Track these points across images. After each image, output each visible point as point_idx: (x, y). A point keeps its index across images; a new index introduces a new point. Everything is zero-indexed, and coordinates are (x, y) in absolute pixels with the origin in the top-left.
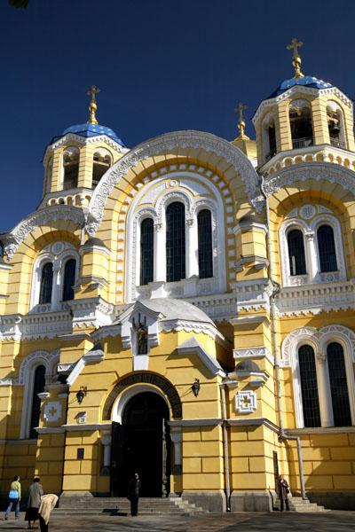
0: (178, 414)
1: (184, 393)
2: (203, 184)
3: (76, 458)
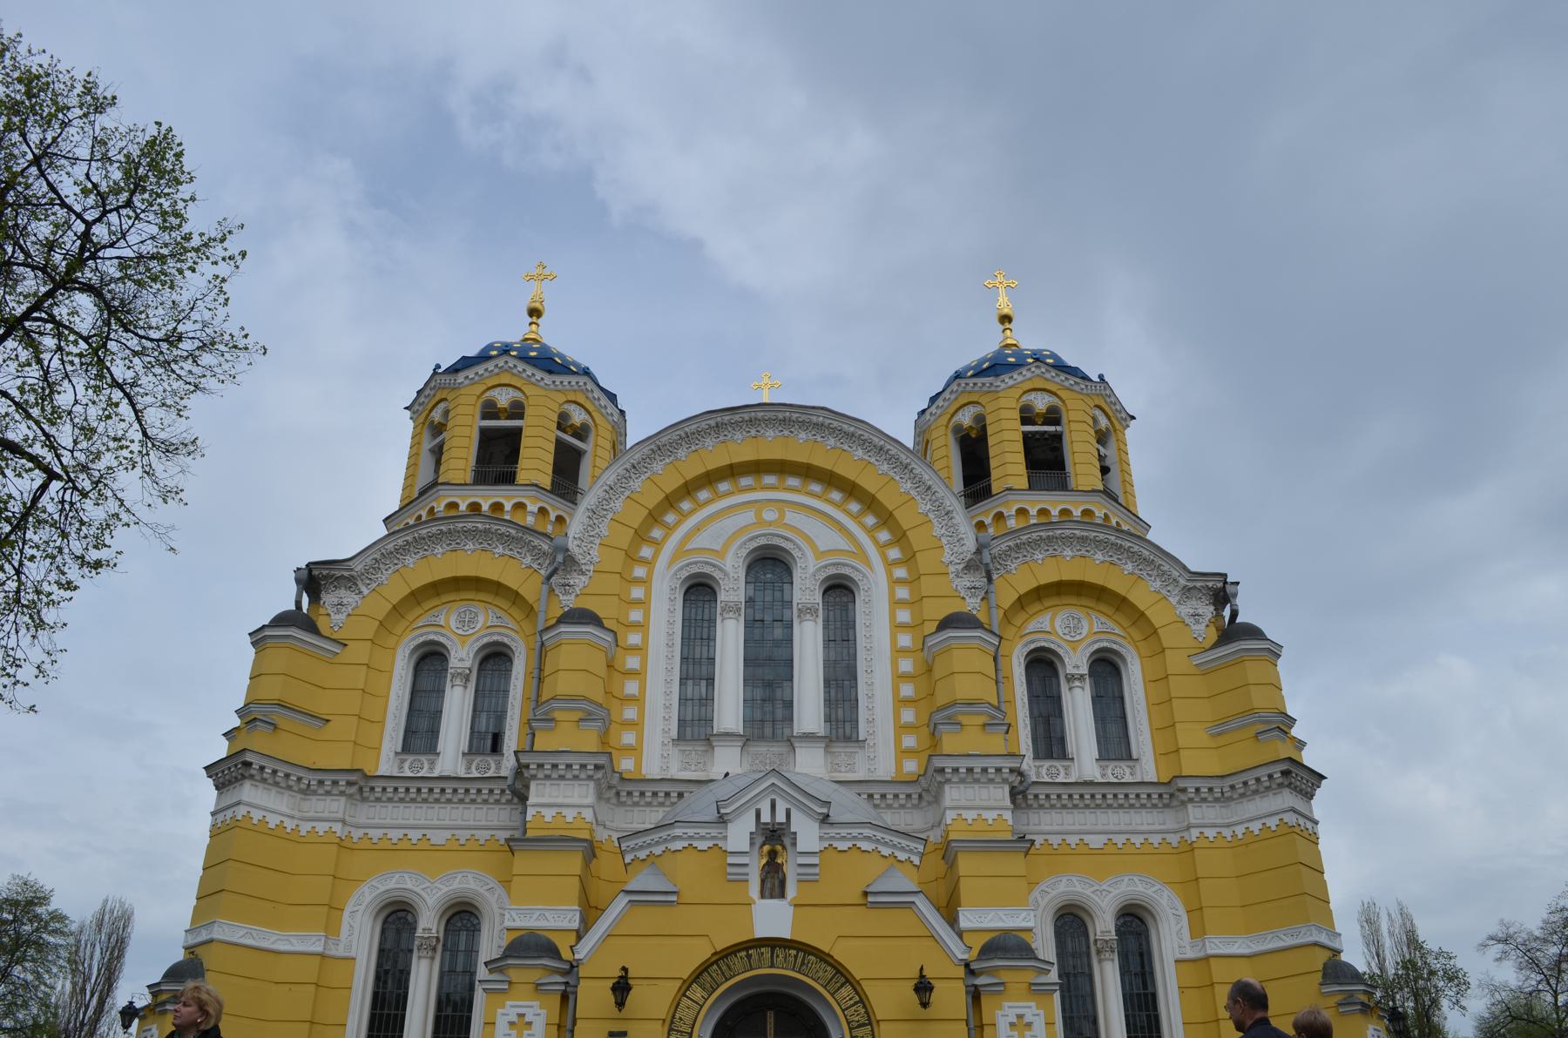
2: (842, 528)
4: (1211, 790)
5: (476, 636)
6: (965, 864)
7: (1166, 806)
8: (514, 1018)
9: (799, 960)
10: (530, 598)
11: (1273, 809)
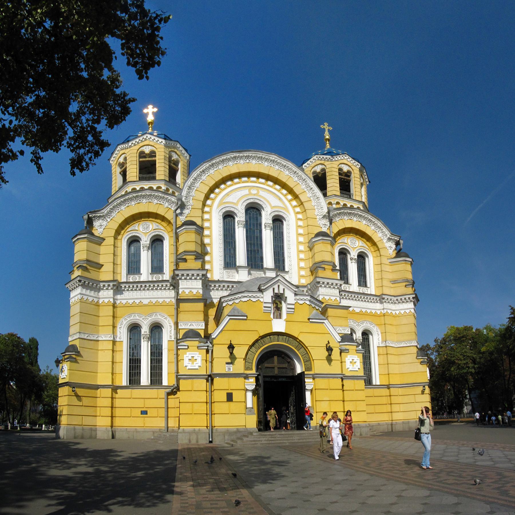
5: (150, 233)
8: (190, 358)
9: (287, 340)
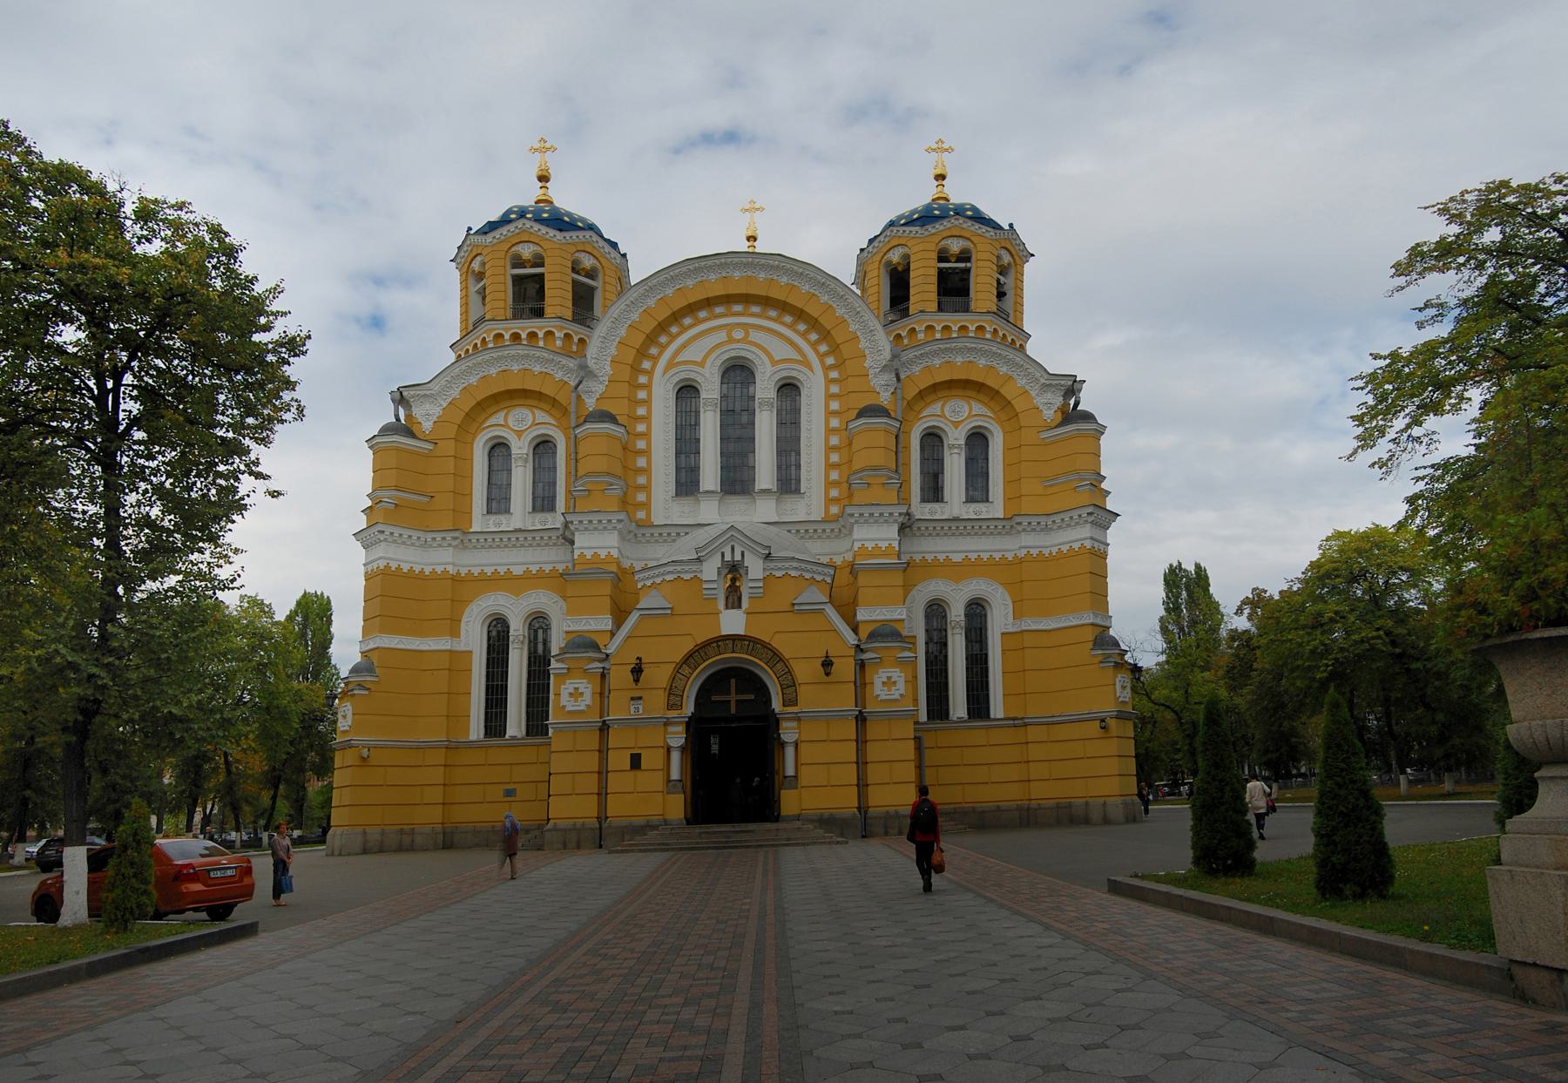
0: (790, 701)
1: (805, 671)
3: (628, 765)
4: (1039, 523)
6: (862, 581)
7: (1007, 533)
8: (572, 691)
9: (751, 647)
10: (564, 403)
11: (1079, 537)
